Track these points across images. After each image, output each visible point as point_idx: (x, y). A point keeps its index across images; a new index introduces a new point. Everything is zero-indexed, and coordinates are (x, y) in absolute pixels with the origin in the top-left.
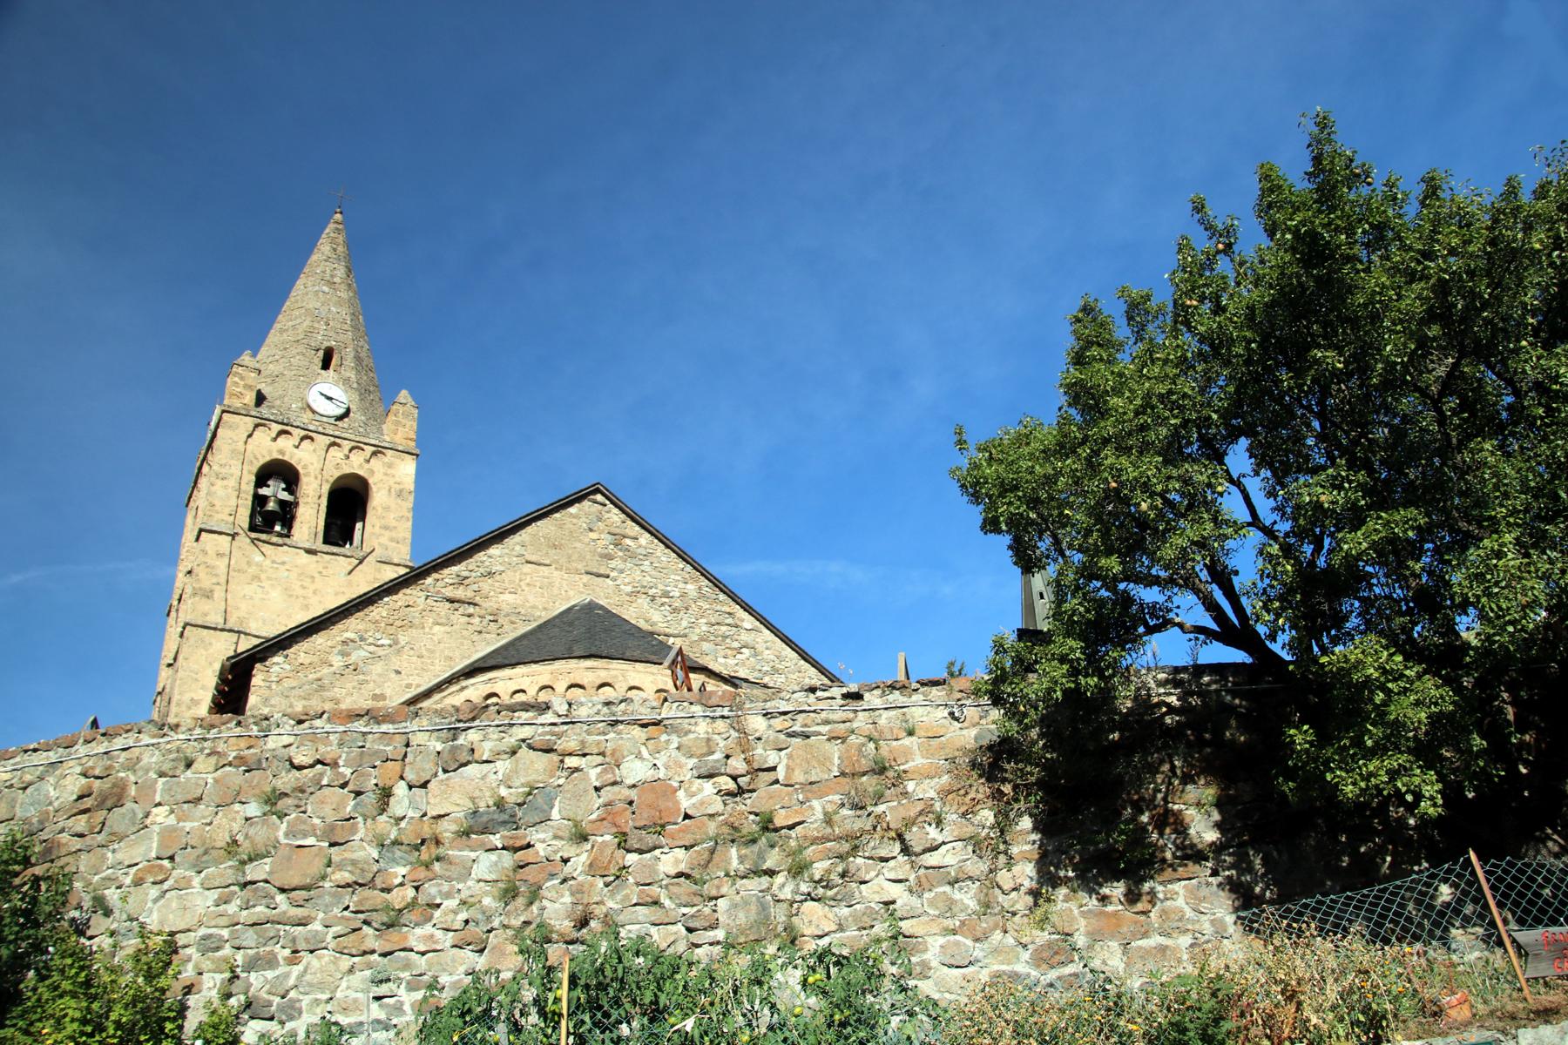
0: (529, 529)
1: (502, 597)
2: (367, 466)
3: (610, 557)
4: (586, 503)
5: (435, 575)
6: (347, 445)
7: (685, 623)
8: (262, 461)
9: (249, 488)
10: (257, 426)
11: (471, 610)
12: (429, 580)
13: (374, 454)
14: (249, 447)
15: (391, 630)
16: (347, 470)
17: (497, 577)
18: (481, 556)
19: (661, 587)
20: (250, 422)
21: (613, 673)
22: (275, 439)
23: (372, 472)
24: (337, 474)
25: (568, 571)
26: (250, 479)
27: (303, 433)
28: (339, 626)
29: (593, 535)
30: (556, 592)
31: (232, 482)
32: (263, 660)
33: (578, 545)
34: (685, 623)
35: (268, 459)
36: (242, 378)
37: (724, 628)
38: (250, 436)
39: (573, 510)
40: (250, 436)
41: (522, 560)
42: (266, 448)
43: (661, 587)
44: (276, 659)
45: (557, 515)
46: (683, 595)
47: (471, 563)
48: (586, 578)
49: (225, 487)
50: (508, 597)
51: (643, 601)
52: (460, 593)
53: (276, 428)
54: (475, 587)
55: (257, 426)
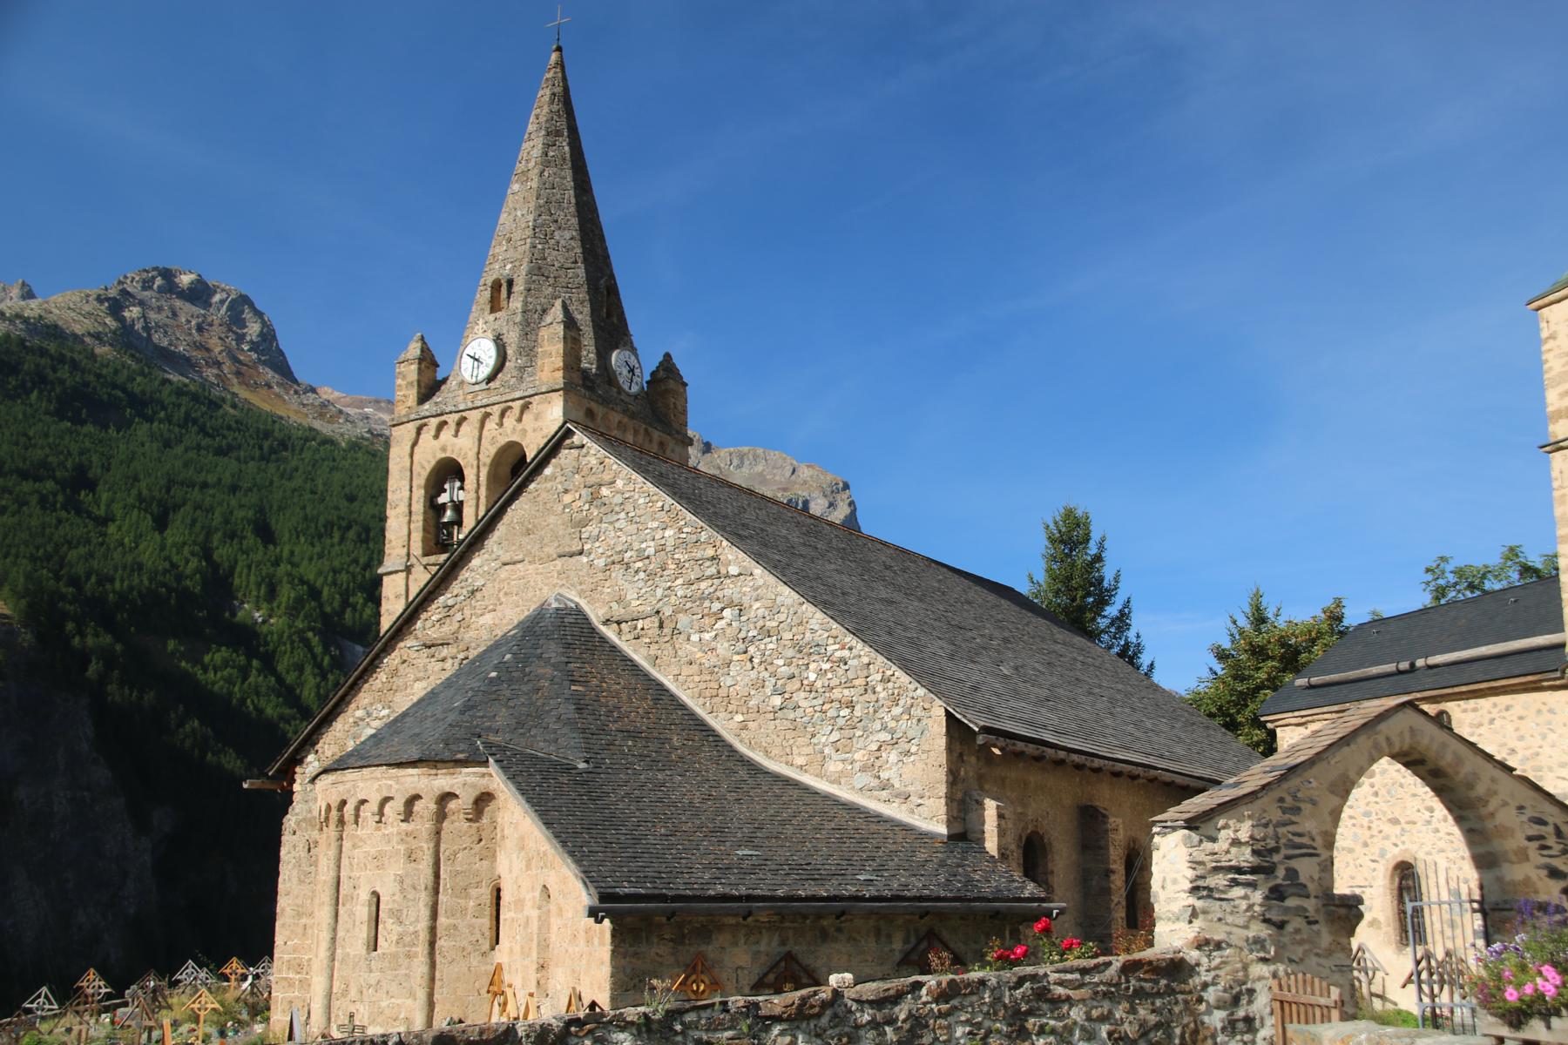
0: (506, 519)
1: (482, 620)
2: (520, 427)
3: (584, 523)
4: (564, 452)
5: (424, 616)
6: (496, 410)
7: (659, 592)
8: (428, 468)
9: (419, 507)
10: (419, 430)
11: (445, 651)
12: (419, 624)
13: (525, 407)
14: (416, 457)
15: (389, 696)
16: (502, 441)
17: (478, 595)
18: (464, 574)
19: (636, 546)
20: (411, 428)
21: (348, 785)
22: (436, 437)
23: (524, 431)
24: (493, 451)
25: (542, 561)
26: (419, 494)
27: (456, 417)
28: (353, 706)
29: (567, 498)
30: (530, 595)
31: (403, 508)
32: (300, 762)
33: (552, 519)
34: (659, 592)
35: (433, 463)
36: (404, 378)
37: (703, 585)
38: (415, 444)
39: (548, 471)
40: (415, 444)
41: (498, 563)
42: (430, 452)
43: (636, 546)
44: (311, 758)
45: (532, 486)
46: (661, 549)
47: (455, 587)
48: (559, 562)
49: (397, 517)
50: (488, 619)
51: (617, 572)
52: (447, 629)
53: (434, 422)
54: (459, 617)
55: (419, 430)
